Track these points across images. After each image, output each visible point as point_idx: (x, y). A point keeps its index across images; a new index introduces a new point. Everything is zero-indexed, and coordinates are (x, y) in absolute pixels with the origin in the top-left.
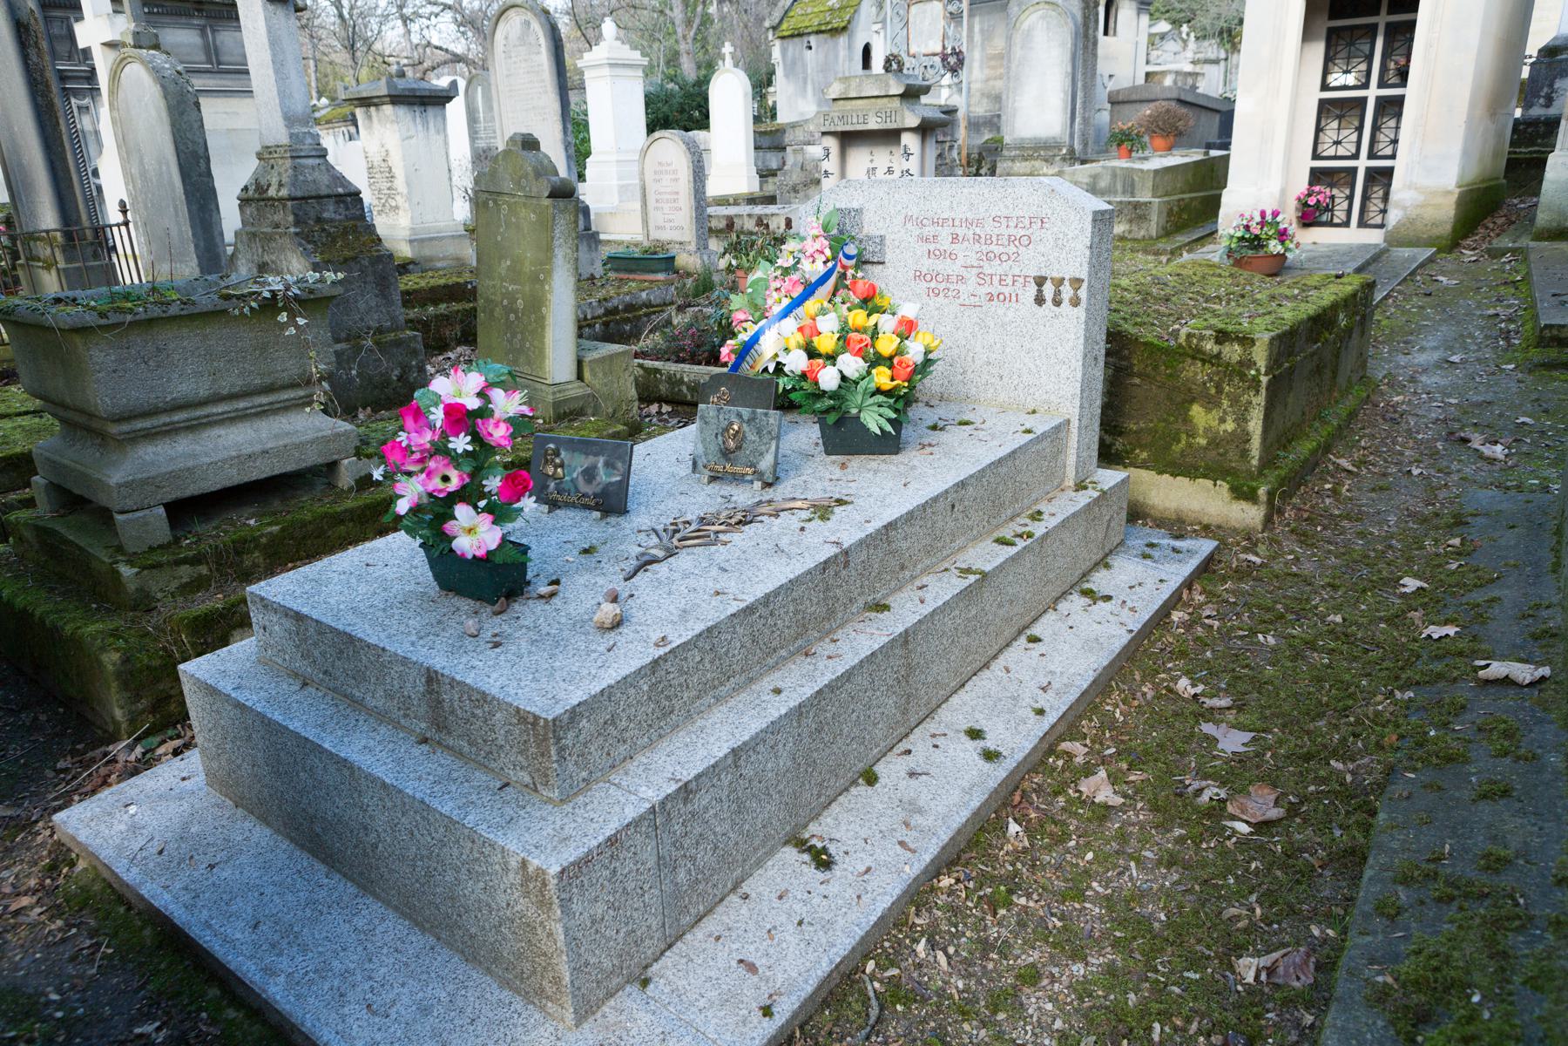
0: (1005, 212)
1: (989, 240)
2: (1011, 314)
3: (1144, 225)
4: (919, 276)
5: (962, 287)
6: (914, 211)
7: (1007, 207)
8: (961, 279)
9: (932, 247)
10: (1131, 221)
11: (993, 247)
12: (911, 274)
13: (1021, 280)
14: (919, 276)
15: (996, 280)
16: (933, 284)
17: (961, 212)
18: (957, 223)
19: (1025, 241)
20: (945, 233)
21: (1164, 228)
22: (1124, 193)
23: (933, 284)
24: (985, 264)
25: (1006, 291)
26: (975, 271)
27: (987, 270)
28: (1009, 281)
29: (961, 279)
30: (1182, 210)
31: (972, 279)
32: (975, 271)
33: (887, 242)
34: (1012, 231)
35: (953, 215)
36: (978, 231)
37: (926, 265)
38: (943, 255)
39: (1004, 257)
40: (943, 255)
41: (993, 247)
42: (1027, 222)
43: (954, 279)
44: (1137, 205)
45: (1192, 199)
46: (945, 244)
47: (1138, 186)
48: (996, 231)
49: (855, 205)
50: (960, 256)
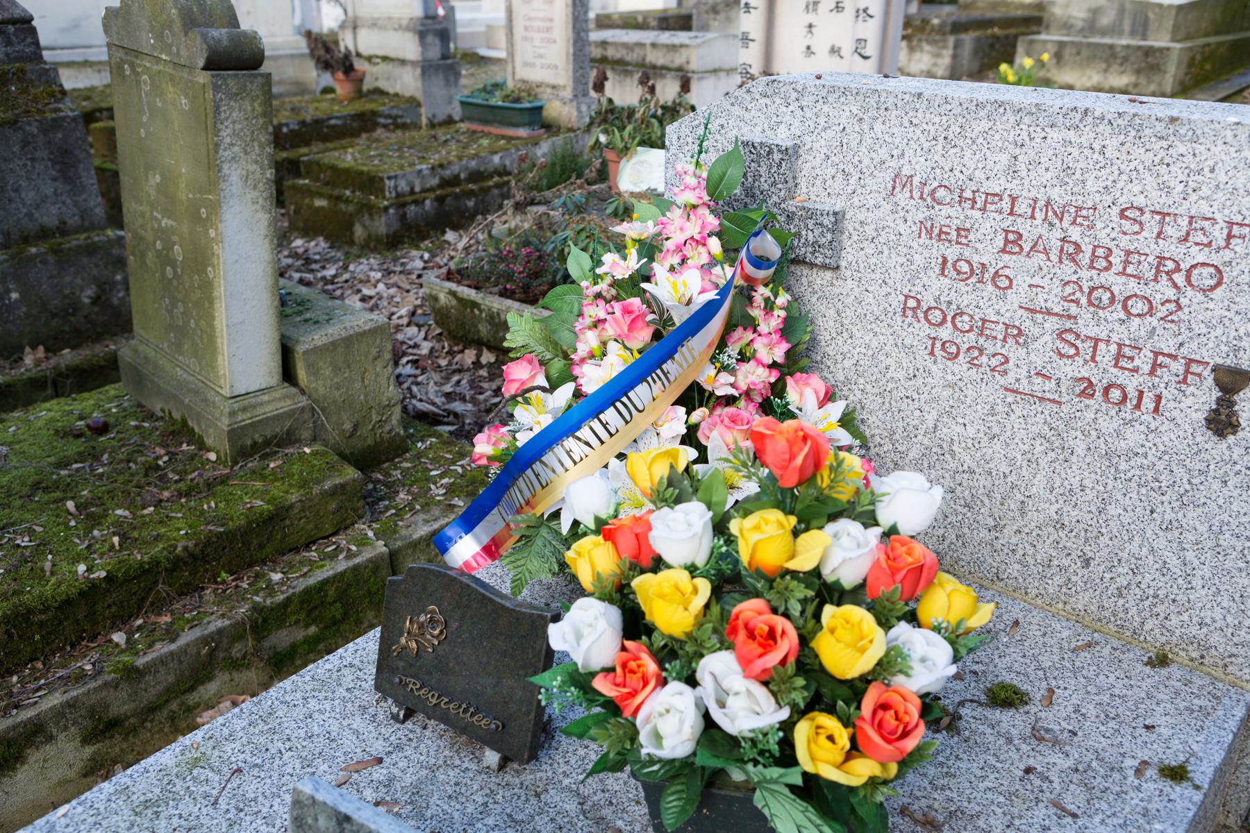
0: (1159, 200)
1: (1102, 258)
2: (1133, 437)
3: (1157, 78)
4: (913, 308)
5: (1011, 350)
6: (917, 166)
7: (1165, 188)
8: (1017, 334)
9: (952, 253)
10: (1138, 72)
11: (1109, 278)
12: (896, 301)
13: (1178, 367)
14: (913, 308)
15: (1106, 354)
16: (945, 333)
17: (1038, 183)
18: (1022, 207)
19: (1204, 277)
20: (987, 230)
21: (1182, 83)
22: (1133, 33)
23: (945, 333)
24: (1085, 315)
25: (1132, 384)
26: (1052, 324)
27: (1087, 325)
28: (1143, 361)
29: (1017, 334)
30: (1205, 59)
31: (1045, 332)
32: (1052, 324)
33: (849, 226)
34: (1171, 248)
35: (1014, 187)
36: (1075, 234)
37: (934, 287)
38: (977, 273)
39: (1138, 307)
40: (977, 273)
41: (1109, 278)
42: (1219, 235)
43: (999, 331)
44: (1148, 52)
45: (1219, 44)
46: (986, 252)
47: (1153, 25)
48: (1124, 242)
49: (782, 137)
50: (1022, 282)
